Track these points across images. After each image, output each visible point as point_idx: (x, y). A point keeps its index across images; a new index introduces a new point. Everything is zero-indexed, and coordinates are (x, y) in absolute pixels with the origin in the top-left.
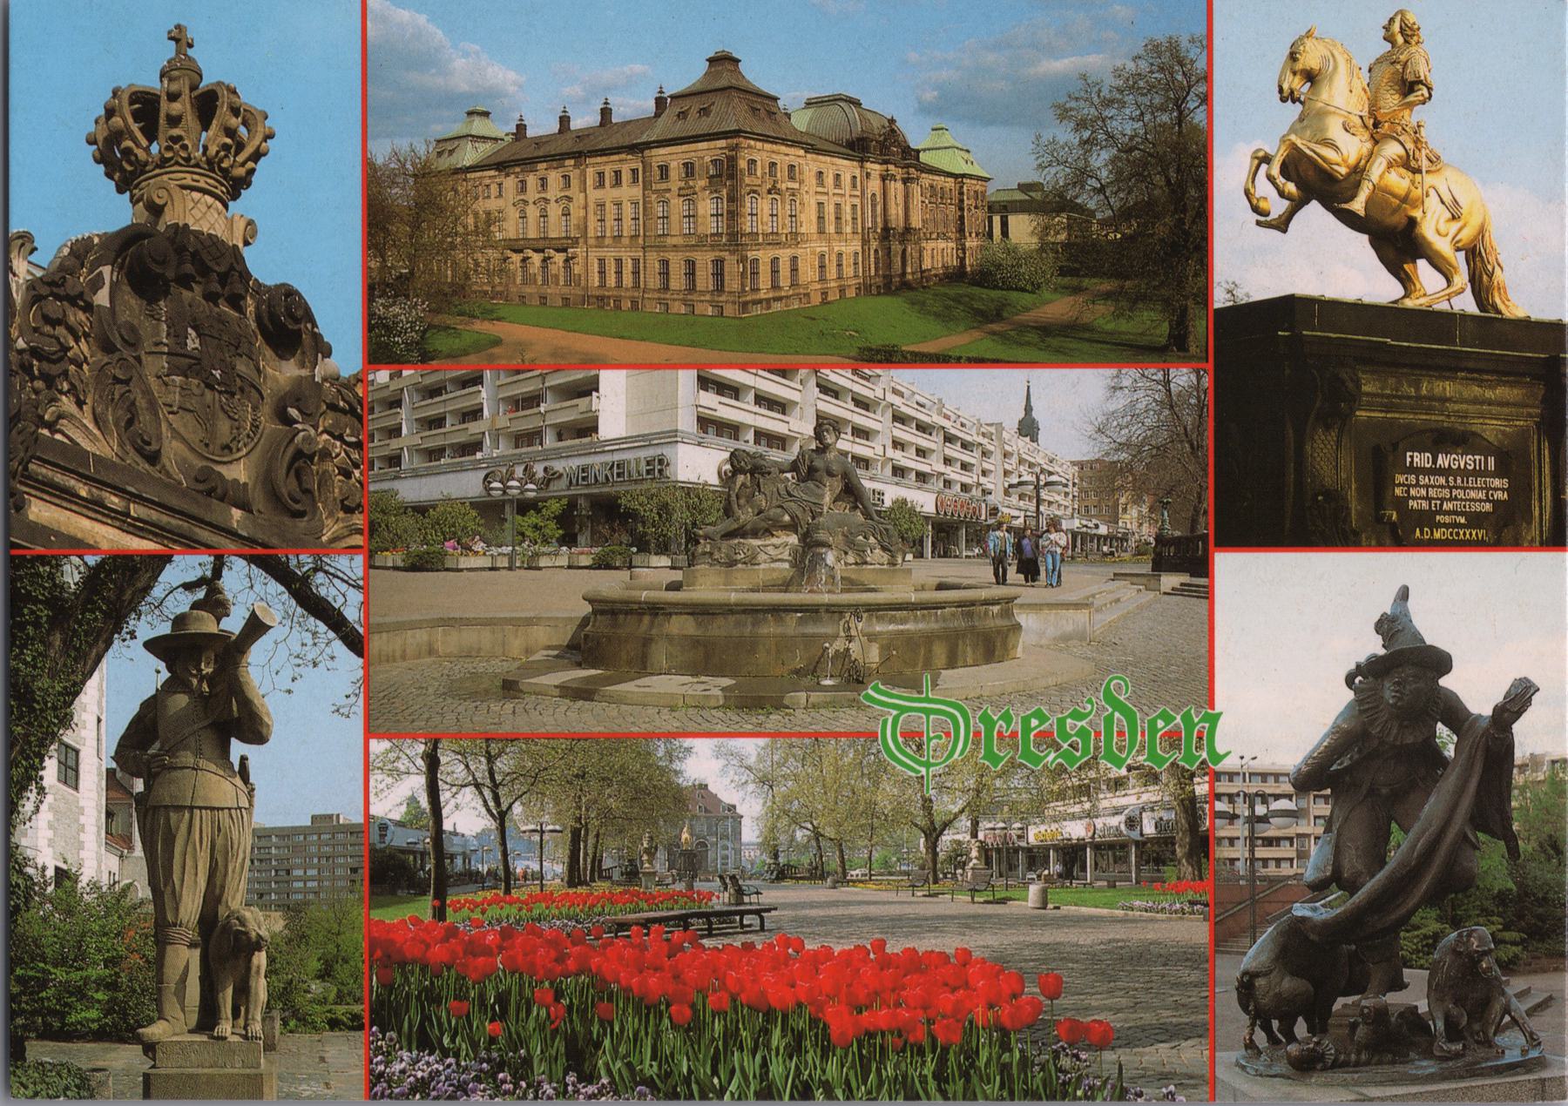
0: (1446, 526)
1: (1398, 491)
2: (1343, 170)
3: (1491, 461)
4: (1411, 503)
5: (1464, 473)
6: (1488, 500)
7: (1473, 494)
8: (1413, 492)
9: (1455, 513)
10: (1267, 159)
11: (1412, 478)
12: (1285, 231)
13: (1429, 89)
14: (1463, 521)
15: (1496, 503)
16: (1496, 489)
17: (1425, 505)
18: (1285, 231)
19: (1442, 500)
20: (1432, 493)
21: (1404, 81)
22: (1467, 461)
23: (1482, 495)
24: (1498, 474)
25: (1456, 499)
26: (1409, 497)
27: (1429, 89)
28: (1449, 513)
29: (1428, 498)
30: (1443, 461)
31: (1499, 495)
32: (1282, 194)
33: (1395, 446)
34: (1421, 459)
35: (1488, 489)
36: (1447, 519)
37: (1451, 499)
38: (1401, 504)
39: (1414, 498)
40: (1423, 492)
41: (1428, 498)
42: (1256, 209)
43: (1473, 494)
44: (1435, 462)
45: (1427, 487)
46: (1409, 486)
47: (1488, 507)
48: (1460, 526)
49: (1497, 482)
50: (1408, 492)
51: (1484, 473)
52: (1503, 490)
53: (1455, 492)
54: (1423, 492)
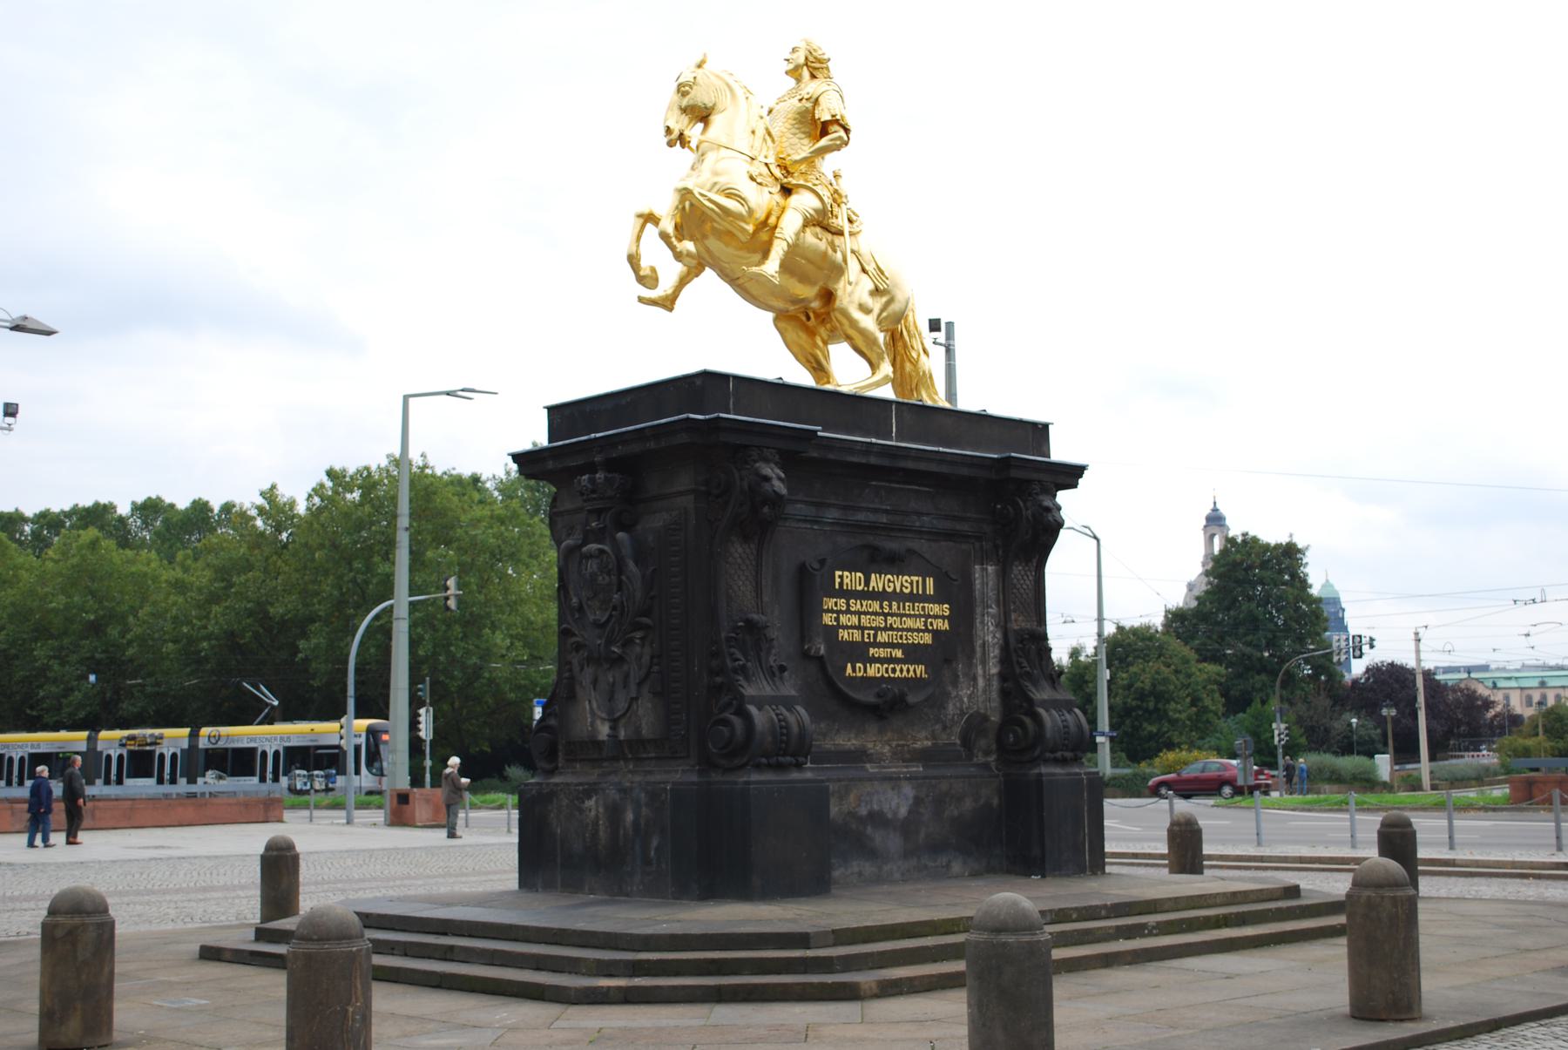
0: (881, 661)
1: (828, 619)
2: (750, 228)
3: (930, 582)
7: (909, 623)
8: (844, 619)
10: (650, 218)
12: (671, 310)
13: (847, 131)
14: (899, 653)
15: (936, 634)
16: (936, 617)
17: (857, 635)
18: (671, 310)
19: (876, 629)
20: (865, 620)
21: (814, 121)
23: (919, 624)
24: (937, 599)
25: (892, 629)
26: (839, 626)
27: (847, 131)
30: (877, 582)
31: (944, 625)
32: (678, 256)
33: (822, 562)
34: (850, 579)
37: (885, 629)
38: (832, 631)
39: (846, 627)
40: (855, 620)
42: (641, 279)
43: (909, 623)
44: (867, 583)
45: (859, 613)
46: (838, 612)
47: (927, 639)
49: (935, 609)
50: (837, 619)
51: (924, 598)
52: (943, 617)
53: (890, 620)
54: (855, 620)
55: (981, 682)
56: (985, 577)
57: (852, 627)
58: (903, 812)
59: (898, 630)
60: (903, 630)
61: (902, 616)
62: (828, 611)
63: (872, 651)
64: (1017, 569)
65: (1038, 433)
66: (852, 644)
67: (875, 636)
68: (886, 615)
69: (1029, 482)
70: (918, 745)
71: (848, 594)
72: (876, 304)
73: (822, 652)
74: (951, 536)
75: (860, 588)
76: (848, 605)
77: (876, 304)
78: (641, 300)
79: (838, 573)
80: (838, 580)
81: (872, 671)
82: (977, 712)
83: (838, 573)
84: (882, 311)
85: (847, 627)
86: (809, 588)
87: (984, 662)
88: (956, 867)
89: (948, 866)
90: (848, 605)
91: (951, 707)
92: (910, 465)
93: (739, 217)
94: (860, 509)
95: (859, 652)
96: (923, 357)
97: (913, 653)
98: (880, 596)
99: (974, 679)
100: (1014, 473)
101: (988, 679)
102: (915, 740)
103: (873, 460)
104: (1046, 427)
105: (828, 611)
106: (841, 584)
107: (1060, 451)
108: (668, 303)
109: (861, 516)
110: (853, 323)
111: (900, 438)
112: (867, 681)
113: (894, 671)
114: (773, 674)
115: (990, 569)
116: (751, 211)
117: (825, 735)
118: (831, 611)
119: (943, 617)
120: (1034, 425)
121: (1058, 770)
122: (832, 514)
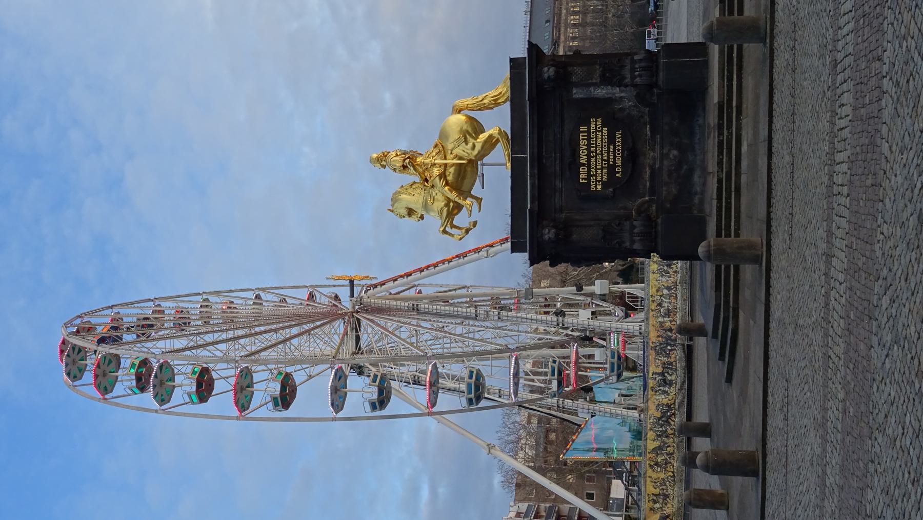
5: (589, 145)
7: (599, 141)
9: (609, 150)
11: (593, 179)
14: (612, 147)
15: (603, 125)
17: (605, 171)
19: (602, 160)
22: (583, 143)
28: (608, 155)
29: (602, 169)
31: (599, 123)
36: (612, 157)
37: (602, 155)
38: (605, 185)
41: (602, 167)
43: (599, 141)
44: (583, 165)
45: (596, 169)
47: (605, 130)
49: (593, 125)
51: (588, 131)
55: (623, 95)
56: (577, 93)
64: (574, 79)
65: (515, 64)
66: (608, 174)
71: (589, 175)
72: (471, 141)
77: (471, 141)
81: (619, 163)
84: (473, 138)
87: (614, 94)
89: (700, 126)
92: (536, 150)
93: (448, 211)
95: (612, 168)
96: (486, 101)
97: (612, 140)
98: (589, 157)
99: (621, 97)
101: (622, 92)
102: (646, 135)
103: (536, 171)
104: (512, 60)
107: (521, 52)
108: (479, 200)
110: (479, 152)
111: (526, 153)
112: (623, 166)
120: (511, 68)
121: (661, 74)
122: (558, 184)
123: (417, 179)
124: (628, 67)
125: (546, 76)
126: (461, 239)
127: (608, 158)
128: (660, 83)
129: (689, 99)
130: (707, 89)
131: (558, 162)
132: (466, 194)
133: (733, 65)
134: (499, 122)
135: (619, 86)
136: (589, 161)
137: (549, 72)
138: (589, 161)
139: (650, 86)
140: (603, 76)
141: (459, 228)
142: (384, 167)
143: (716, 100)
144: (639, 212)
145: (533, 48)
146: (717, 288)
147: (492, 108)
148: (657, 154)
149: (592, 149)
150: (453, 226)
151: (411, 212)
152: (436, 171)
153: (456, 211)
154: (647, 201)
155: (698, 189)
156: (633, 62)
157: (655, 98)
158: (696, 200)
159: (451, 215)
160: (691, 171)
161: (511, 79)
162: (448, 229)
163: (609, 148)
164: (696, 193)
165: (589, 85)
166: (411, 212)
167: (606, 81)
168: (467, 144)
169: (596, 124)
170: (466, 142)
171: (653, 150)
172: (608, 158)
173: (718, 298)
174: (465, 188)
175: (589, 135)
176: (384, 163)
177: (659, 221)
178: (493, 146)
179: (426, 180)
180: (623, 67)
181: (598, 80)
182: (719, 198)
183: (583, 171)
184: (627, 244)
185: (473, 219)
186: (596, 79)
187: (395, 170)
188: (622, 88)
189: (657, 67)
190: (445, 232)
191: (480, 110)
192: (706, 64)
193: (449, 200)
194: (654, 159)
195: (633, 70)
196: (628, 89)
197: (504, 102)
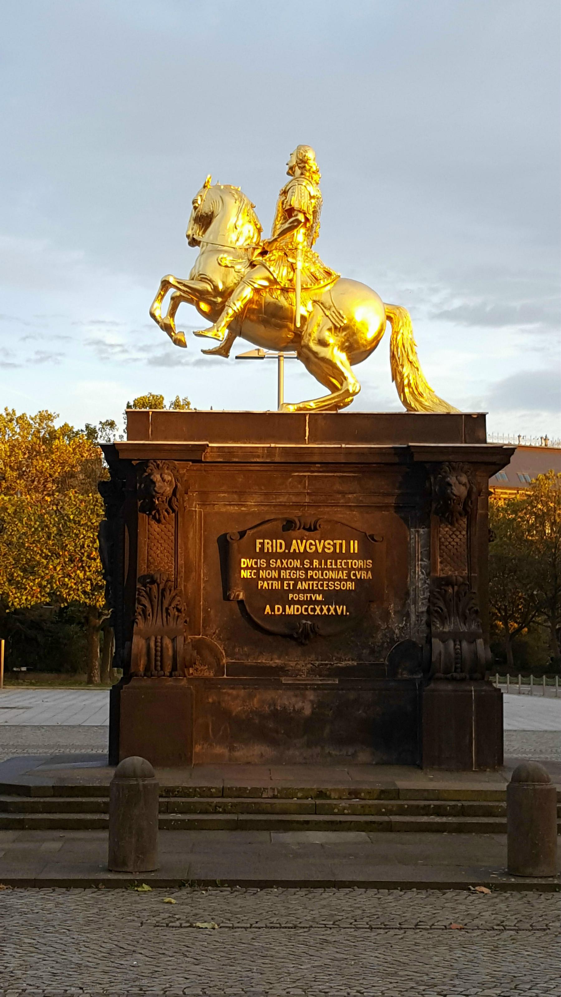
0: (299, 602)
3: (354, 546)
4: (260, 583)
5: (323, 556)
6: (350, 579)
7: (331, 575)
9: (313, 592)
11: (262, 562)
14: (320, 598)
15: (359, 582)
17: (276, 585)
19: (296, 581)
23: (343, 575)
25: (312, 579)
26: (258, 578)
28: (304, 591)
29: (280, 579)
30: (297, 546)
31: (363, 575)
35: (349, 570)
36: (302, 597)
37: (306, 580)
39: (263, 580)
40: (275, 574)
41: (280, 579)
43: (331, 575)
45: (279, 569)
46: (258, 569)
47: (350, 586)
48: (317, 602)
49: (360, 563)
50: (257, 574)
51: (349, 555)
52: (367, 570)
53: (310, 573)
54: (275, 574)
55: (413, 618)
57: (271, 579)
58: (308, 711)
59: (318, 580)
60: (324, 580)
61: (323, 570)
62: (247, 568)
63: (291, 596)
66: (272, 591)
67: (295, 585)
68: (306, 570)
69: (441, 463)
70: (343, 664)
71: (269, 556)
73: (241, 596)
74: (380, 508)
75: (279, 550)
76: (268, 563)
78: (204, 352)
79: (258, 541)
80: (258, 546)
81: (290, 611)
82: (409, 641)
83: (258, 541)
85: (267, 579)
86: (227, 552)
87: (415, 603)
88: (364, 756)
89: (354, 755)
90: (268, 563)
91: (379, 636)
92: (316, 459)
94: (281, 494)
95: (279, 597)
97: (332, 597)
99: (408, 615)
100: (417, 458)
102: (340, 660)
104: (482, 417)
105: (247, 568)
106: (262, 549)
109: (282, 499)
110: (315, 354)
111: (313, 439)
112: (284, 617)
113: (314, 610)
114: (168, 614)
115: (421, 531)
116: (216, 288)
117: (248, 656)
118: (246, 568)
119: (367, 570)
120: (468, 416)
121: (450, 687)
123: (267, 236)
124: (464, 628)
125: (452, 479)
126: (153, 316)
127: (300, 591)
128: (432, 686)
129: (401, 735)
130: (420, 767)
131: (294, 499)
132: (237, 328)
133: (461, 818)
134: (372, 390)
135: (428, 611)
136: (295, 556)
137: (459, 486)
138: (295, 556)
139: (427, 668)
140: (448, 581)
141: (172, 313)
142: (291, 171)
143: (403, 784)
144: (198, 646)
145: (503, 455)
146: (58, 791)
147: (394, 378)
148: (303, 679)
149: (316, 563)
150: (175, 302)
151: (204, 220)
152: (281, 273)
153: (204, 307)
154: (219, 660)
155: (237, 754)
156: (472, 638)
157: (406, 676)
158: (219, 750)
159: (195, 296)
160: (273, 742)
161: (448, 415)
162: (171, 291)
163: (319, 592)
164: (232, 749)
165: (429, 555)
166: (204, 220)
167: (440, 585)
168: (330, 330)
169: (362, 568)
170: (336, 329)
171: (312, 672)
172: (300, 591)
173: (41, 791)
174: (248, 326)
175: (341, 556)
176: (298, 171)
177: (184, 682)
178: (325, 380)
179: (264, 253)
180: (465, 619)
181: (439, 574)
182: (223, 793)
183: (278, 546)
184: (140, 625)
185: (190, 339)
186: (442, 570)
187: (285, 193)
188: (424, 618)
189: (463, 680)
190: (166, 285)
191: (393, 356)
192: (463, 766)
193: (227, 294)
194: (296, 673)
195: (457, 637)
196: (424, 627)
197: (405, 402)
